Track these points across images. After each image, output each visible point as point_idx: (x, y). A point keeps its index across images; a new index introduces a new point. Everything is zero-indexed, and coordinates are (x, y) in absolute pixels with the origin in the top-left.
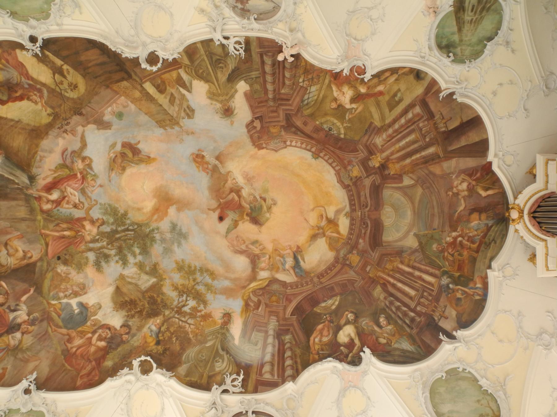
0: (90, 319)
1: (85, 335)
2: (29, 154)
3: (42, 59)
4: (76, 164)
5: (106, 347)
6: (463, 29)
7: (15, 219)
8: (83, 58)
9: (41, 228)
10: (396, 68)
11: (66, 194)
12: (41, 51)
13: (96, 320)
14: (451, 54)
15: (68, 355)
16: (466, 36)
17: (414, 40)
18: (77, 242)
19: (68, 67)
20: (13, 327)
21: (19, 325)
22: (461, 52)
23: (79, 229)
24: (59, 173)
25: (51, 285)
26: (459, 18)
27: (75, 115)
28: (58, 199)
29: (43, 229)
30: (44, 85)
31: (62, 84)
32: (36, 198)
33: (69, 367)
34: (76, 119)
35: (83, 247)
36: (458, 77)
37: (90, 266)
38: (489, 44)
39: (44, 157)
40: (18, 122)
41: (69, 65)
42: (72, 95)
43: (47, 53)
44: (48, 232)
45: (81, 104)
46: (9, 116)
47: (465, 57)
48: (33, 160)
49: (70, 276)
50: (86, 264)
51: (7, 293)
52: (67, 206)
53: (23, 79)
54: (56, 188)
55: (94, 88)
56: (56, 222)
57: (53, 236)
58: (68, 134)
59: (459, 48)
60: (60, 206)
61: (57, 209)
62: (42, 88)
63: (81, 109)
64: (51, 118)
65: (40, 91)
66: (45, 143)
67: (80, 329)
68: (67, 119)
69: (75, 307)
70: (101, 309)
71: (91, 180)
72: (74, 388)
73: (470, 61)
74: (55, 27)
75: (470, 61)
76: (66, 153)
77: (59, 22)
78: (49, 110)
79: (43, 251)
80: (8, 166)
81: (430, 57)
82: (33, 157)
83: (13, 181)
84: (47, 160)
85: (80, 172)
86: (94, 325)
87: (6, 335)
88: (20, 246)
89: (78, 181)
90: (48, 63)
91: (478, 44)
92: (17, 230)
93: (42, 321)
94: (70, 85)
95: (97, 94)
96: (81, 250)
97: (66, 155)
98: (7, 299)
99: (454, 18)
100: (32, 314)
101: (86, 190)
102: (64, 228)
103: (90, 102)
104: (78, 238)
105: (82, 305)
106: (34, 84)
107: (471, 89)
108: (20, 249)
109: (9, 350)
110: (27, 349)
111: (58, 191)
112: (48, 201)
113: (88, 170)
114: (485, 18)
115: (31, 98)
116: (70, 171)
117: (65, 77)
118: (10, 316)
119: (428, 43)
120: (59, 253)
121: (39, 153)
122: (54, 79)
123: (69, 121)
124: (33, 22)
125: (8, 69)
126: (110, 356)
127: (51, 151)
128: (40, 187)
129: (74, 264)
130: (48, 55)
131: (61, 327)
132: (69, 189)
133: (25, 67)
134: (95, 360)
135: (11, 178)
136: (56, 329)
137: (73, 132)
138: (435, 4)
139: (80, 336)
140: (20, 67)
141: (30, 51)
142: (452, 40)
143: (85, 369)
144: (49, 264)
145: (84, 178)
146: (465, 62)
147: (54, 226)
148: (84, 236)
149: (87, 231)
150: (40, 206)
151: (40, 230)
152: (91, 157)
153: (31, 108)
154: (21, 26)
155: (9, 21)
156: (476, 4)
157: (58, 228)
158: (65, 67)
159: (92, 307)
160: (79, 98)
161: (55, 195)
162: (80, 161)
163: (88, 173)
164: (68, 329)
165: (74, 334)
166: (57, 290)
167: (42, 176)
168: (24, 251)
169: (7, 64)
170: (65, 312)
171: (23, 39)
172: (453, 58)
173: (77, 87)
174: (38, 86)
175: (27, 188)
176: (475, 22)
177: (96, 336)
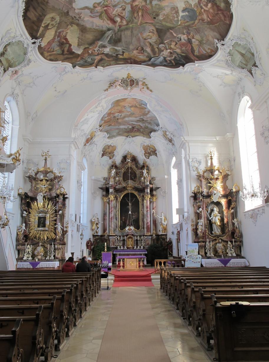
0: (192, 8)
1: (202, 13)
2: (95, 32)
3: (42, 36)
4: (98, 11)
5: (212, 4)
7: (131, 35)
8: (35, 19)
9: (136, 25)
11: (117, 14)
12: (39, 39)
13: (194, 5)
15: (211, 23)
18: (146, 9)
19: (43, 24)
20: (189, 41)
21: (188, 39)
23: (138, 8)
24: (105, 18)
25: (170, 23)
27: (69, 15)
28: (120, 18)
29: (137, 24)
30: (56, 32)
31: (53, 24)
32: (120, 27)
33: (218, 24)
34: (71, 14)
35: (149, 6)
37: (160, 3)
39: (96, 25)
40: (79, 38)
41: (42, 24)
42: (58, 19)
43: (38, 35)
44: (139, 22)
45: (62, 13)
46: (77, 41)
48: (99, 30)
49: (166, 14)
50: (159, 5)
51: (171, 41)
52: (124, 14)
53: (55, 41)
54: (114, 19)
55: (51, 9)
56: (133, 19)
57: (142, 20)
58: (81, 16)
60: (124, 16)
61: (126, 18)
62: (58, 32)
63: (65, 13)
64: (73, 25)
65: (60, 33)
66: (88, 26)
67: (198, 14)
68: (72, 18)
69: (185, 14)
70: (189, 1)
71: (107, 2)
72: (230, 26)
74: (24, 37)
76: (93, 16)
77: (20, 36)
78: (69, 27)
79: (150, 25)
80: (104, 39)
82: (97, 30)
83: (111, 37)
84: (98, 24)
85: (103, 8)
86: (197, 7)
87: (192, 45)
88: (145, 35)
89: (108, 9)
90: (44, 33)
92: (138, 35)
93: (189, 30)
94: (52, 21)
95: (54, 7)
96: (151, 7)
97: (94, 15)
98: (174, 41)
100: (184, 33)
101: (114, 4)
102: (137, 15)
103: (60, 9)
104: (143, 9)
105: (184, 11)
106: (57, 36)
108: (148, 34)
109: (200, 45)
110: (202, 38)
111: (115, 18)
112: (121, 22)
113: (101, 4)
115: (65, 35)
116: (103, 13)
117: (48, 24)
118: (183, 41)
120: (152, 18)
121: (94, 28)
122: (51, 28)
123: (73, 17)
124: (25, 46)
125: (53, 47)
126: (218, 3)
127: (93, 22)
128: (114, 26)
129: (159, 11)
130: (40, 34)
131: (195, 22)
132: (114, 13)
133: (49, 41)
134: (218, 11)
135: (109, 38)
136: (195, 24)
137: (79, 14)
139: (202, 15)
140: (49, 43)
141: (41, 44)
143: (221, 17)
144: (157, 23)
145: (106, 6)
147: (136, 19)
148: (142, 6)
149: (139, 4)
150: (124, 26)
151: (138, 25)
152: (93, 4)
153: (70, 34)
154: (30, 49)
155: (29, 54)
157: (137, 18)
158: (43, 25)
159: (186, 6)
160: (59, 15)
161: (118, 19)
162: (96, 9)
163: (103, 4)
164: (196, 19)
165: (200, 17)
166: (173, 21)
167: (107, 25)
168: (149, 33)
169: (50, 48)
170: (186, 19)
171: (36, 47)
173: (53, 17)
174: (58, 34)
175: (114, 31)
177: (204, 7)
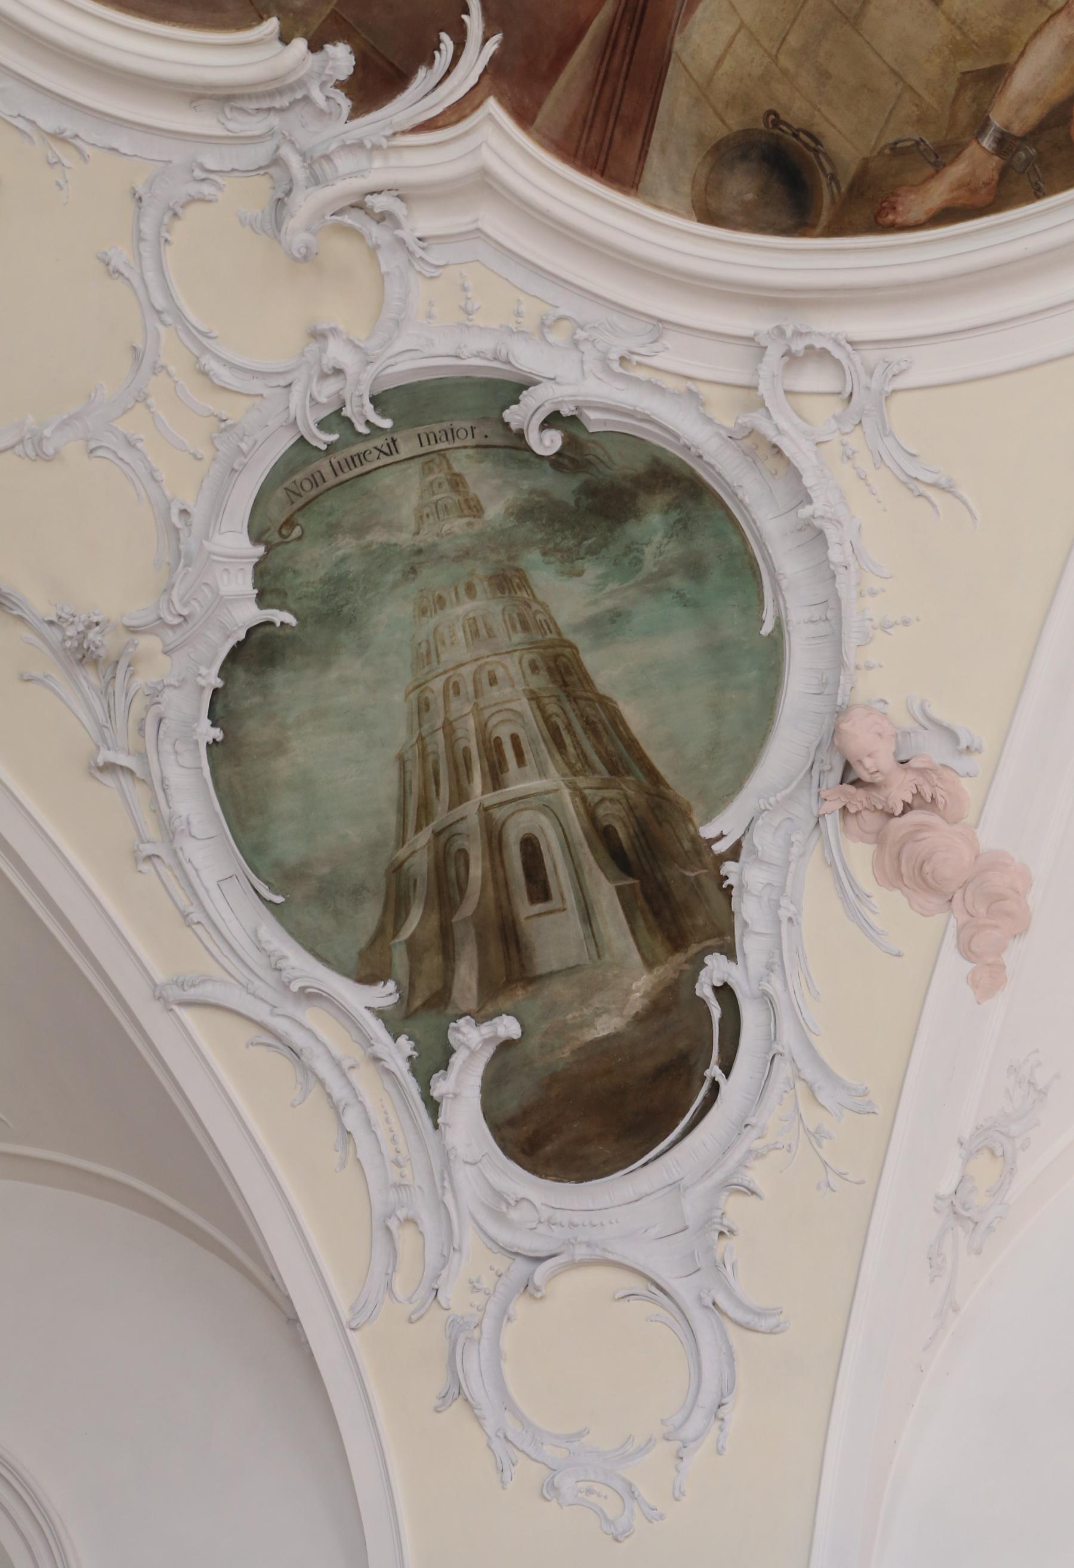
6: (540, 681)
10: (1038, 194)
14: (547, 443)
16: (475, 631)
17: (947, 489)
22: (456, 482)
26: (615, 768)
36: (389, 262)
38: (250, 614)
47: (407, 448)
59: (495, 511)
73: (337, 420)
75: (337, 420)
81: (743, 378)
91: (337, 582)
99: (659, 760)
107: (208, 175)
114: (392, 819)
119: (817, 507)
138: (880, 839)
142: (592, 570)
146: (377, 401)
156: (524, 909)
172: (513, 416)
176: (460, 767)
